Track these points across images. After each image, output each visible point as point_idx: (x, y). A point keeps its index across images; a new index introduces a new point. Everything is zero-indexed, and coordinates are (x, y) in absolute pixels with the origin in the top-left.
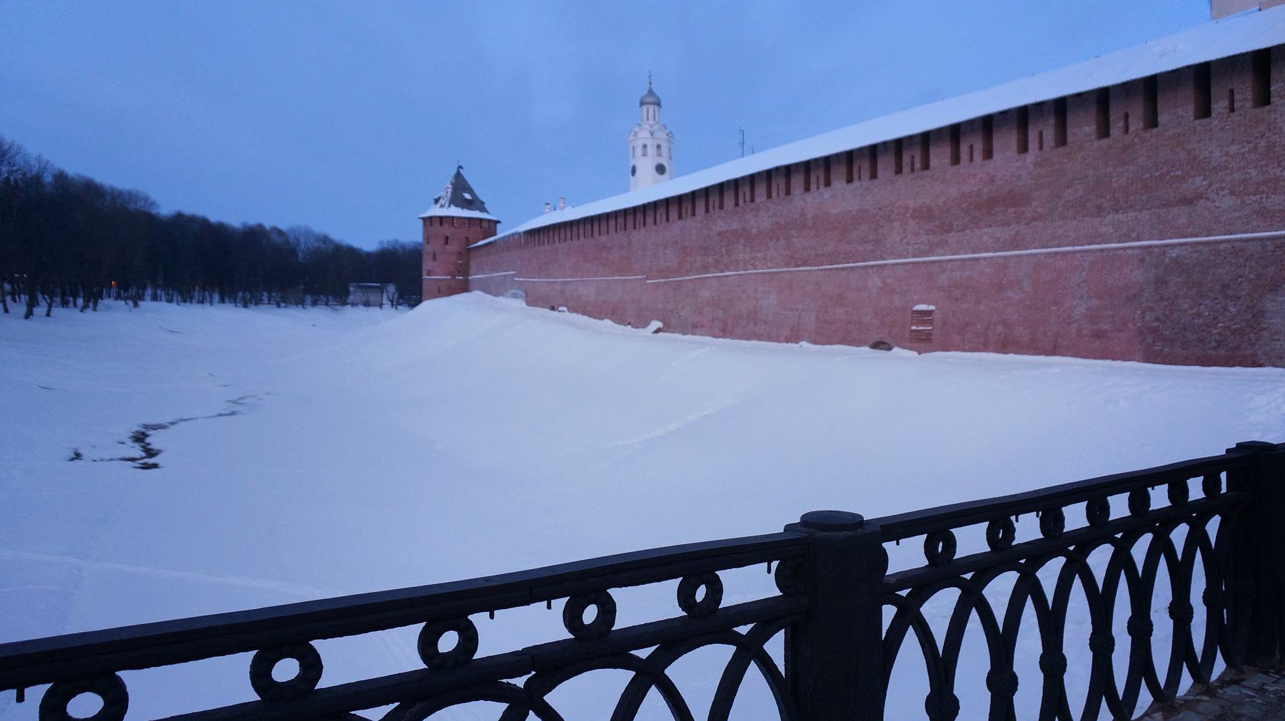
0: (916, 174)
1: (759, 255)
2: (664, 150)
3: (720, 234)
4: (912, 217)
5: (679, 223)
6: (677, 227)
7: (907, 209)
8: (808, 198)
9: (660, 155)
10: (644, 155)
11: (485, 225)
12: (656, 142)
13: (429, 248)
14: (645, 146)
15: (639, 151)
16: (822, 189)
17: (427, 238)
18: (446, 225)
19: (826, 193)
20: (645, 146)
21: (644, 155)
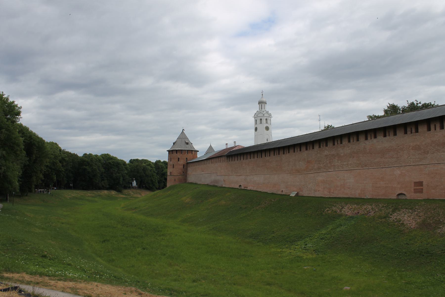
0: (413, 134)
1: (345, 163)
2: (268, 121)
3: (326, 156)
4: (412, 149)
5: (306, 152)
6: (305, 154)
7: (410, 146)
8: (367, 142)
9: (267, 123)
10: (261, 123)
11: (193, 152)
12: (265, 118)
13: (171, 163)
14: (261, 119)
15: (258, 121)
16: (373, 139)
17: (170, 159)
18: (178, 153)
19: (375, 141)
20: (261, 119)
21: (261, 123)
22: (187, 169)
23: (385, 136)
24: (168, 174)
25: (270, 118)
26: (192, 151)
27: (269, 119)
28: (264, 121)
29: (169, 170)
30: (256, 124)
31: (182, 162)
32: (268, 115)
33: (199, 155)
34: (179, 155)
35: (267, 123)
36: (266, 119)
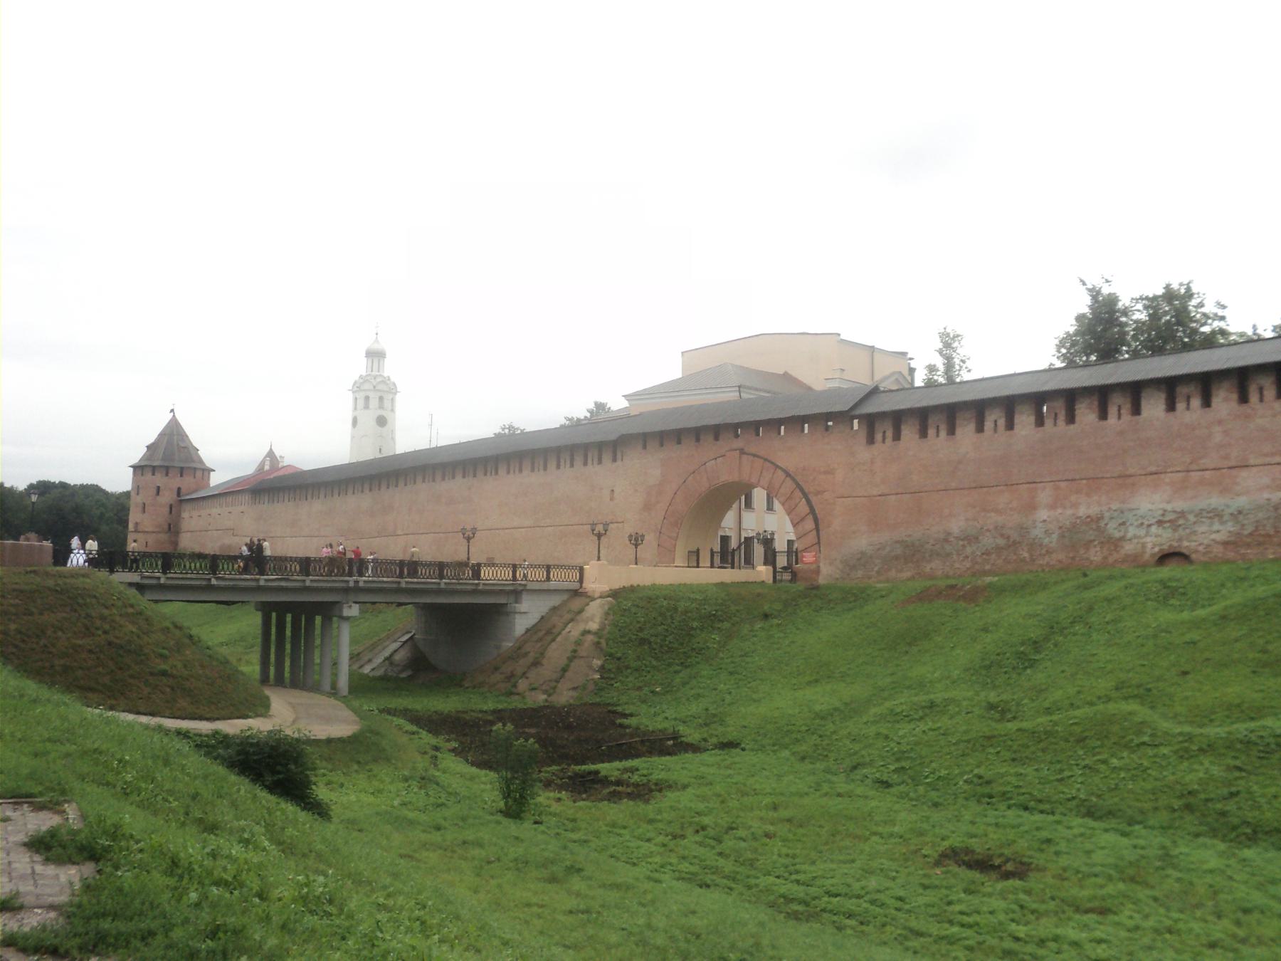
2: (387, 404)
9: (381, 407)
10: (367, 407)
11: (199, 474)
12: (379, 394)
14: (367, 398)
15: (361, 403)
21: (367, 407)
22: (179, 515)
23: (464, 477)
24: (131, 527)
25: (390, 396)
26: (195, 469)
27: (388, 397)
28: (374, 403)
29: (134, 517)
30: (355, 409)
31: (167, 497)
32: (385, 388)
33: (216, 479)
34: (159, 479)
35: (381, 407)
36: (381, 399)
